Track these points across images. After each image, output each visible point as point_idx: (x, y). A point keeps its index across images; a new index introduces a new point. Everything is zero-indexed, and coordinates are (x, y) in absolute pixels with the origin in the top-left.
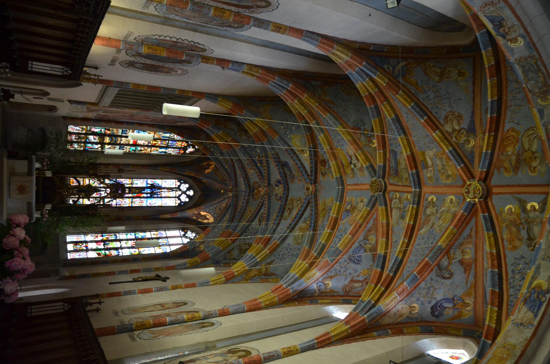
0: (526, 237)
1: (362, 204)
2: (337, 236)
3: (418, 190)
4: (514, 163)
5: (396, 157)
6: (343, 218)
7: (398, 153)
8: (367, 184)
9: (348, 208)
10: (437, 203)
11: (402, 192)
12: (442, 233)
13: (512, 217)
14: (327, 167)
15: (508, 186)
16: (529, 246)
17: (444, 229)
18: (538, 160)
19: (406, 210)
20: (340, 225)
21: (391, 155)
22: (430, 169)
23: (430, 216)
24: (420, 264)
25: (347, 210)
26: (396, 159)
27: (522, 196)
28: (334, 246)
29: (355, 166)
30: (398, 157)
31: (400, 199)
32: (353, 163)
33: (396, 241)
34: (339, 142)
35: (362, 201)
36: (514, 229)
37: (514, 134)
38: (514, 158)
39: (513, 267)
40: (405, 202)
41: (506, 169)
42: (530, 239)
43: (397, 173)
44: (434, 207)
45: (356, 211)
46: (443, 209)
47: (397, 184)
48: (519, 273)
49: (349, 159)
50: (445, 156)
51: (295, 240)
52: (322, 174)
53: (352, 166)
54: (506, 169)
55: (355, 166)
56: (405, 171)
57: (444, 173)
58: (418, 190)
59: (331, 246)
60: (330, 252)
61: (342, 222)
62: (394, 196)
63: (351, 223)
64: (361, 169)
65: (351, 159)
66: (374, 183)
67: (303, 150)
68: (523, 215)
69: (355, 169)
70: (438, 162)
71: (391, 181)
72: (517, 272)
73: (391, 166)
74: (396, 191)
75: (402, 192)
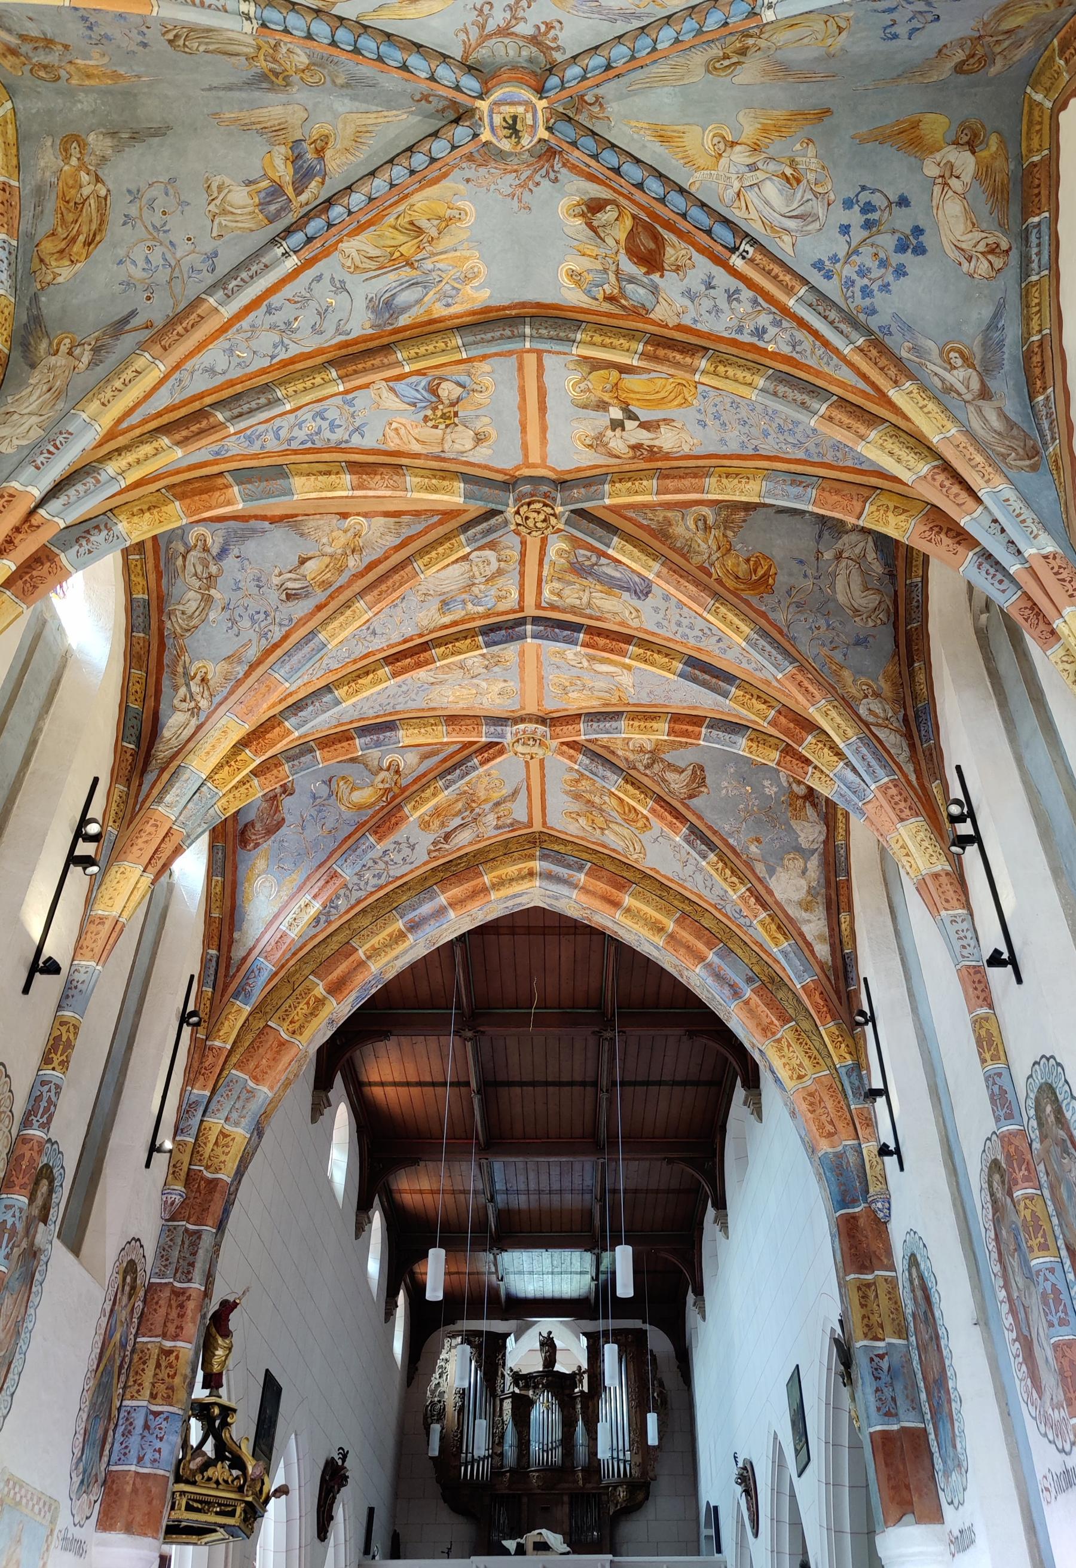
0: (448, 829)
1: (469, 444)
2: (320, 415)
3: (529, 628)
4: (587, 796)
5: (628, 590)
6: (400, 386)
7: (636, 603)
8: (544, 458)
9: (448, 390)
10: (496, 669)
11: (522, 574)
12: (424, 705)
13: (482, 794)
14: (629, 267)
15: (543, 776)
16: (434, 843)
17: (432, 705)
18: (589, 829)
19: (470, 606)
20: (371, 392)
21: (637, 579)
22: (585, 664)
23: (462, 668)
24: (342, 724)
25: (434, 392)
26: (621, 588)
27: (523, 795)
28: (283, 433)
29: (617, 425)
30: (626, 595)
31: (500, 572)
32: (630, 425)
33: (374, 633)
34: (717, 417)
35: (479, 439)
36: (460, 805)
37: (640, 824)
38: (597, 800)
39: (393, 846)
40: (493, 592)
41: (577, 781)
42: (447, 837)
43: (579, 570)
44: (486, 667)
45: (439, 432)
46: (484, 684)
47: (546, 560)
48: (386, 863)
49: (644, 415)
50: (614, 701)
51: (192, 30)
52: (595, 207)
53: (616, 413)
54: (577, 781)
55: (617, 425)
56: (585, 600)
57: (571, 684)
58: (529, 628)
59: (278, 422)
60: (258, 444)
61: (385, 393)
62: (508, 552)
63: (391, 434)
64: (598, 443)
65: (645, 425)
66: (544, 521)
67: (743, 52)
68: (487, 807)
69: (601, 420)
70: (601, 684)
71: (557, 546)
72: (386, 858)
73: (603, 561)
74: (523, 555)
75: (522, 574)
